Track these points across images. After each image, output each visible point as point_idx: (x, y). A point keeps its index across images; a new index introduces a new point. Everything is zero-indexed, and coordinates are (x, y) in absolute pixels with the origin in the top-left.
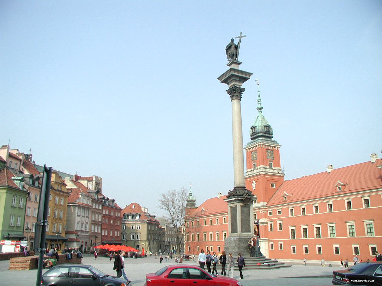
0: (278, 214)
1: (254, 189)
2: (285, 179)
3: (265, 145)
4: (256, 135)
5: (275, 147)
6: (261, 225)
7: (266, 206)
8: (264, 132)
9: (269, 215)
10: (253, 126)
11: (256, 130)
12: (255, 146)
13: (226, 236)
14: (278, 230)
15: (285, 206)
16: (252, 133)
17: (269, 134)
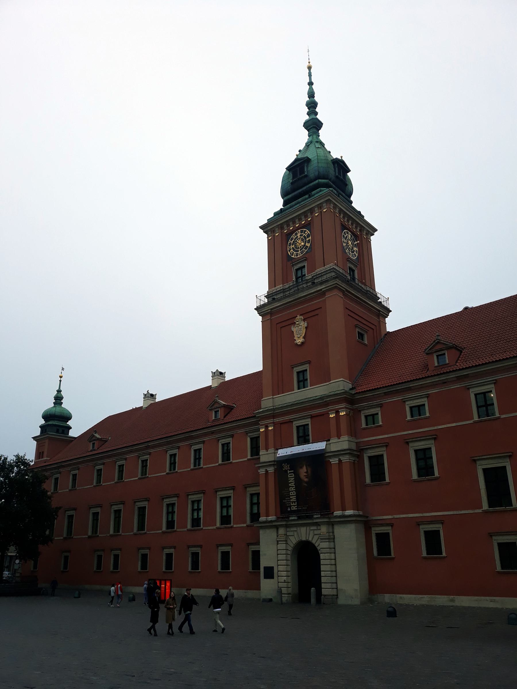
0: (409, 418)
1: (299, 341)
2: (393, 324)
3: (341, 211)
4: (304, 188)
5: (362, 229)
6: (334, 461)
7: (353, 392)
8: (333, 178)
9: (364, 426)
10: (296, 160)
11: (307, 171)
12: (305, 214)
13: (173, 512)
14: (415, 476)
15: (444, 383)
16: (292, 183)
17: (344, 192)
